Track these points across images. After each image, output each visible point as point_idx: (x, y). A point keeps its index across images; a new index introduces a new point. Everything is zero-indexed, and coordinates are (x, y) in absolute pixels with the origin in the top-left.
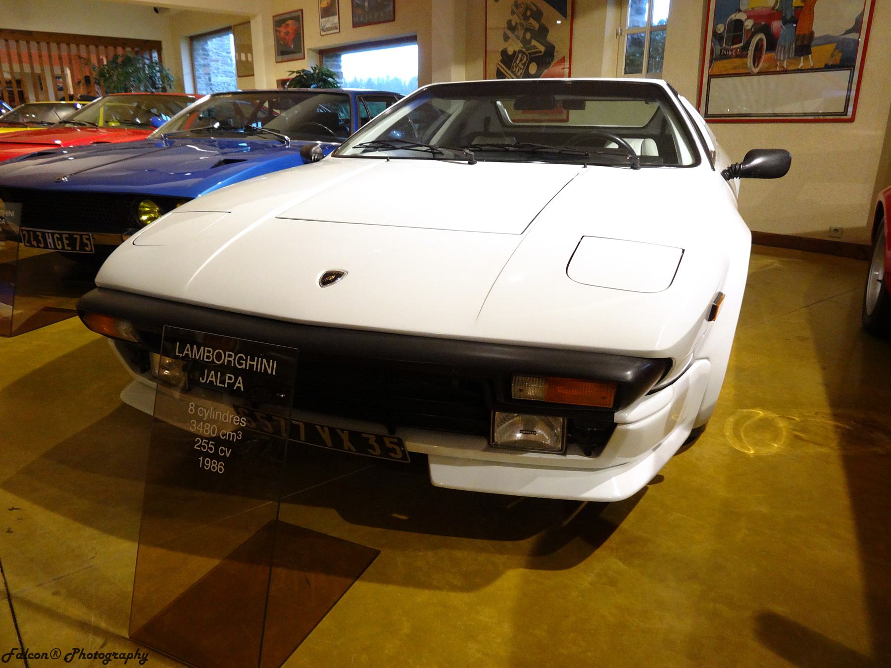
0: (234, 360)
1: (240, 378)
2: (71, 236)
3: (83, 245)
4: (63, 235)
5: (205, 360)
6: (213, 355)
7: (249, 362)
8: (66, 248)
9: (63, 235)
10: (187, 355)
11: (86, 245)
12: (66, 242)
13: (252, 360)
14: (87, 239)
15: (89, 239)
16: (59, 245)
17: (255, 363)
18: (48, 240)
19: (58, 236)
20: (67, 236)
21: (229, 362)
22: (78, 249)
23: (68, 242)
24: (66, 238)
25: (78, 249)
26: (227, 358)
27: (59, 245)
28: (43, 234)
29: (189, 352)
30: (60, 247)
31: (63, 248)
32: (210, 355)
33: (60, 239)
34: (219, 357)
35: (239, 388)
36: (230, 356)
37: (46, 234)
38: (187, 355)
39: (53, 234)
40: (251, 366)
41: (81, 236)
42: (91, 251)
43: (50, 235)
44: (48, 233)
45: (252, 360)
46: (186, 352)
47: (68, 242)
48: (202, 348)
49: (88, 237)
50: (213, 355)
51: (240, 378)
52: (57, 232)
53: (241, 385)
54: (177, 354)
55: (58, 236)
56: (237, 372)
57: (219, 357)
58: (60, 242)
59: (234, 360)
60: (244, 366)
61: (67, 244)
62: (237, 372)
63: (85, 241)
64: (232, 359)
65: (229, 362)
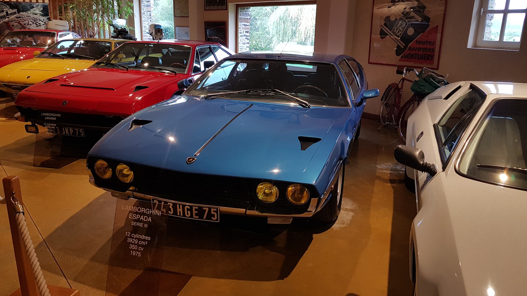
2: (200, 208)
3: (210, 216)
4: (193, 207)
8: (194, 216)
9: (193, 207)
11: (214, 216)
12: (195, 212)
14: (214, 211)
15: (217, 212)
16: (188, 214)
18: (178, 210)
19: (189, 208)
20: (197, 208)
22: (205, 217)
23: (197, 212)
24: (196, 210)
25: (205, 217)
27: (188, 214)
28: (174, 205)
30: (189, 215)
31: (192, 216)
33: (191, 209)
37: (178, 205)
39: (184, 206)
41: (210, 209)
42: (217, 220)
43: (181, 206)
44: (179, 205)
47: (197, 212)
49: (216, 210)
52: (188, 204)
55: (189, 208)
58: (189, 212)
61: (196, 213)
63: (213, 213)
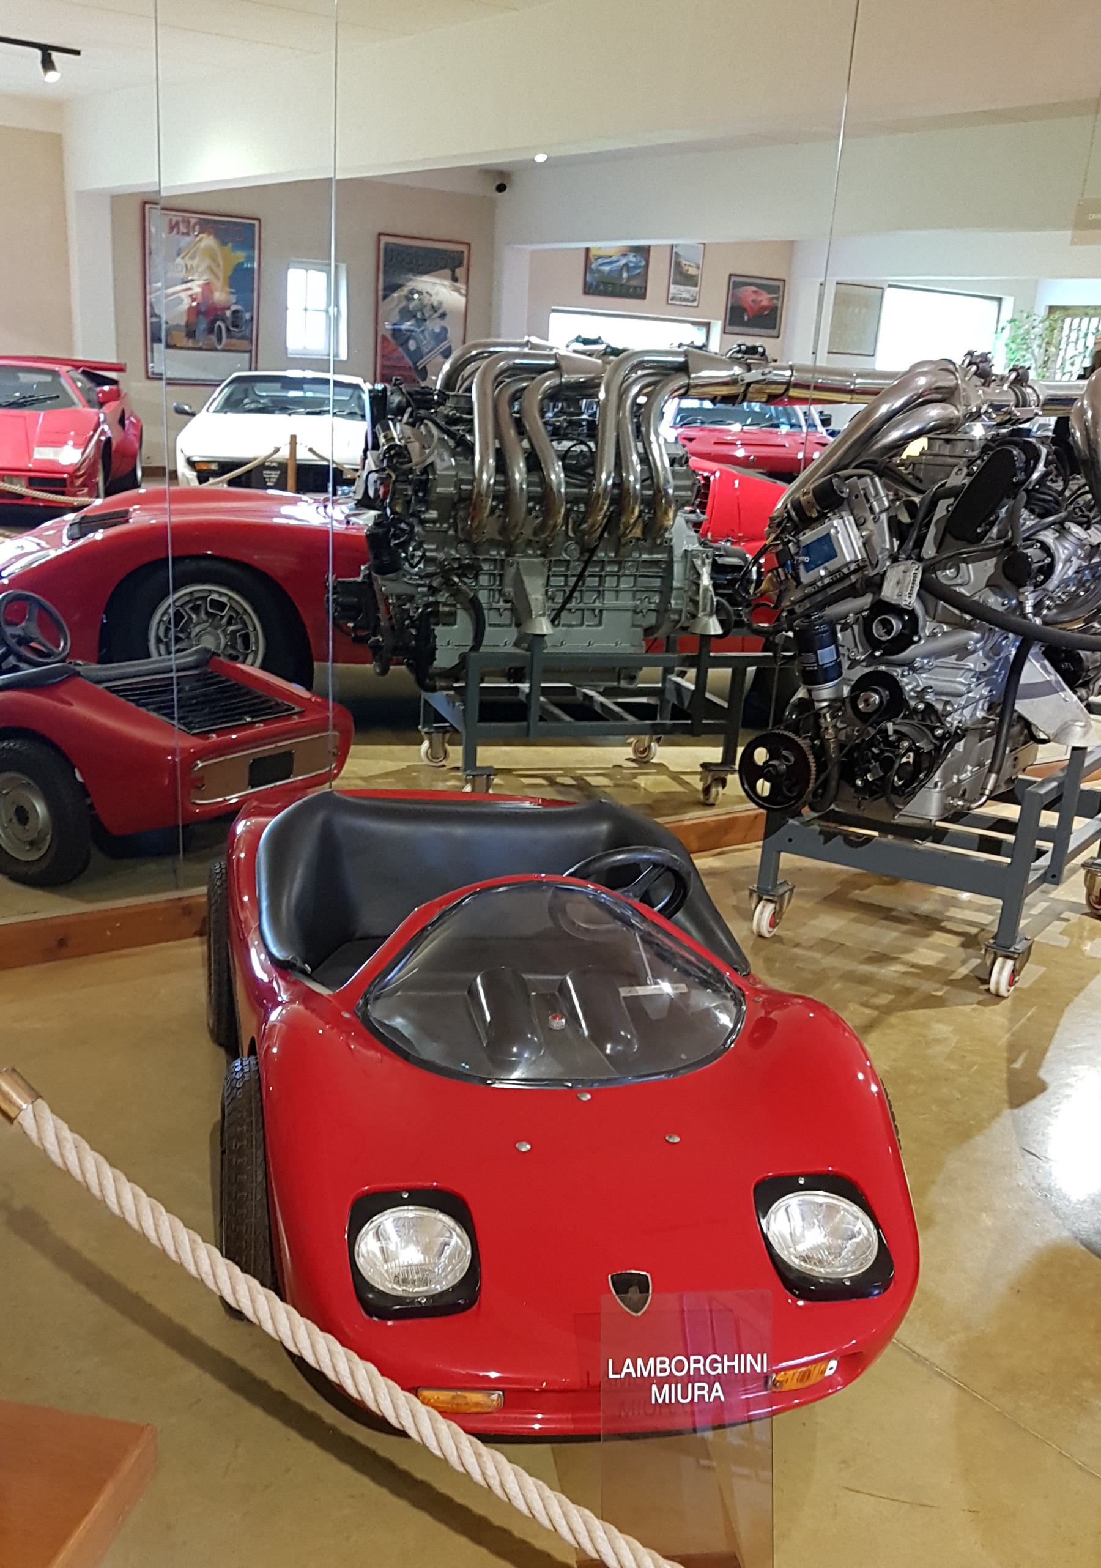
0: (704, 1365)
1: (717, 1385)
5: (659, 1374)
6: (670, 1365)
7: (727, 1364)
10: (628, 1374)
13: (731, 1359)
17: (736, 1363)
21: (697, 1370)
26: (693, 1366)
29: (632, 1370)
32: (666, 1366)
34: (680, 1366)
35: (717, 1398)
36: (697, 1361)
38: (628, 1374)
40: (731, 1368)
45: (731, 1359)
46: (625, 1370)
48: (652, 1360)
50: (670, 1365)
51: (717, 1385)
53: (720, 1394)
54: (611, 1376)
56: (711, 1381)
57: (680, 1366)
59: (704, 1365)
60: (719, 1371)
62: (711, 1381)
64: (700, 1366)
65: (697, 1370)
